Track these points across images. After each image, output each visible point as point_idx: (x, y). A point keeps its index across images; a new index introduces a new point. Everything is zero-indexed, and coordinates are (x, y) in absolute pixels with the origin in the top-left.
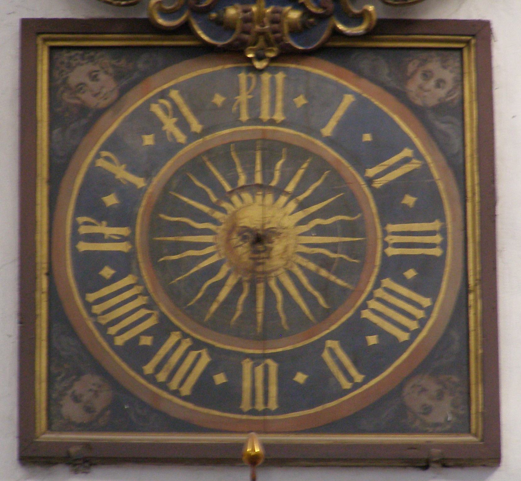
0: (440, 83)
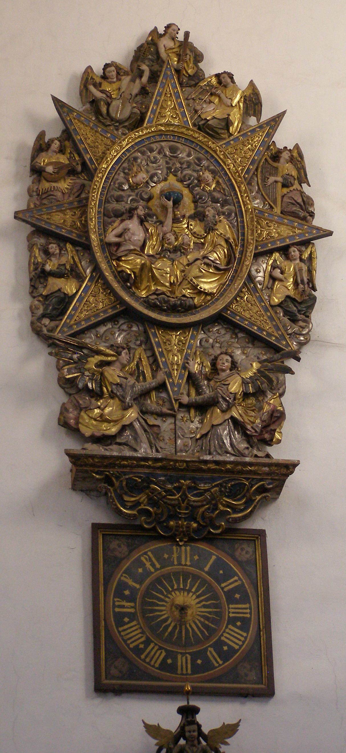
0: (247, 552)
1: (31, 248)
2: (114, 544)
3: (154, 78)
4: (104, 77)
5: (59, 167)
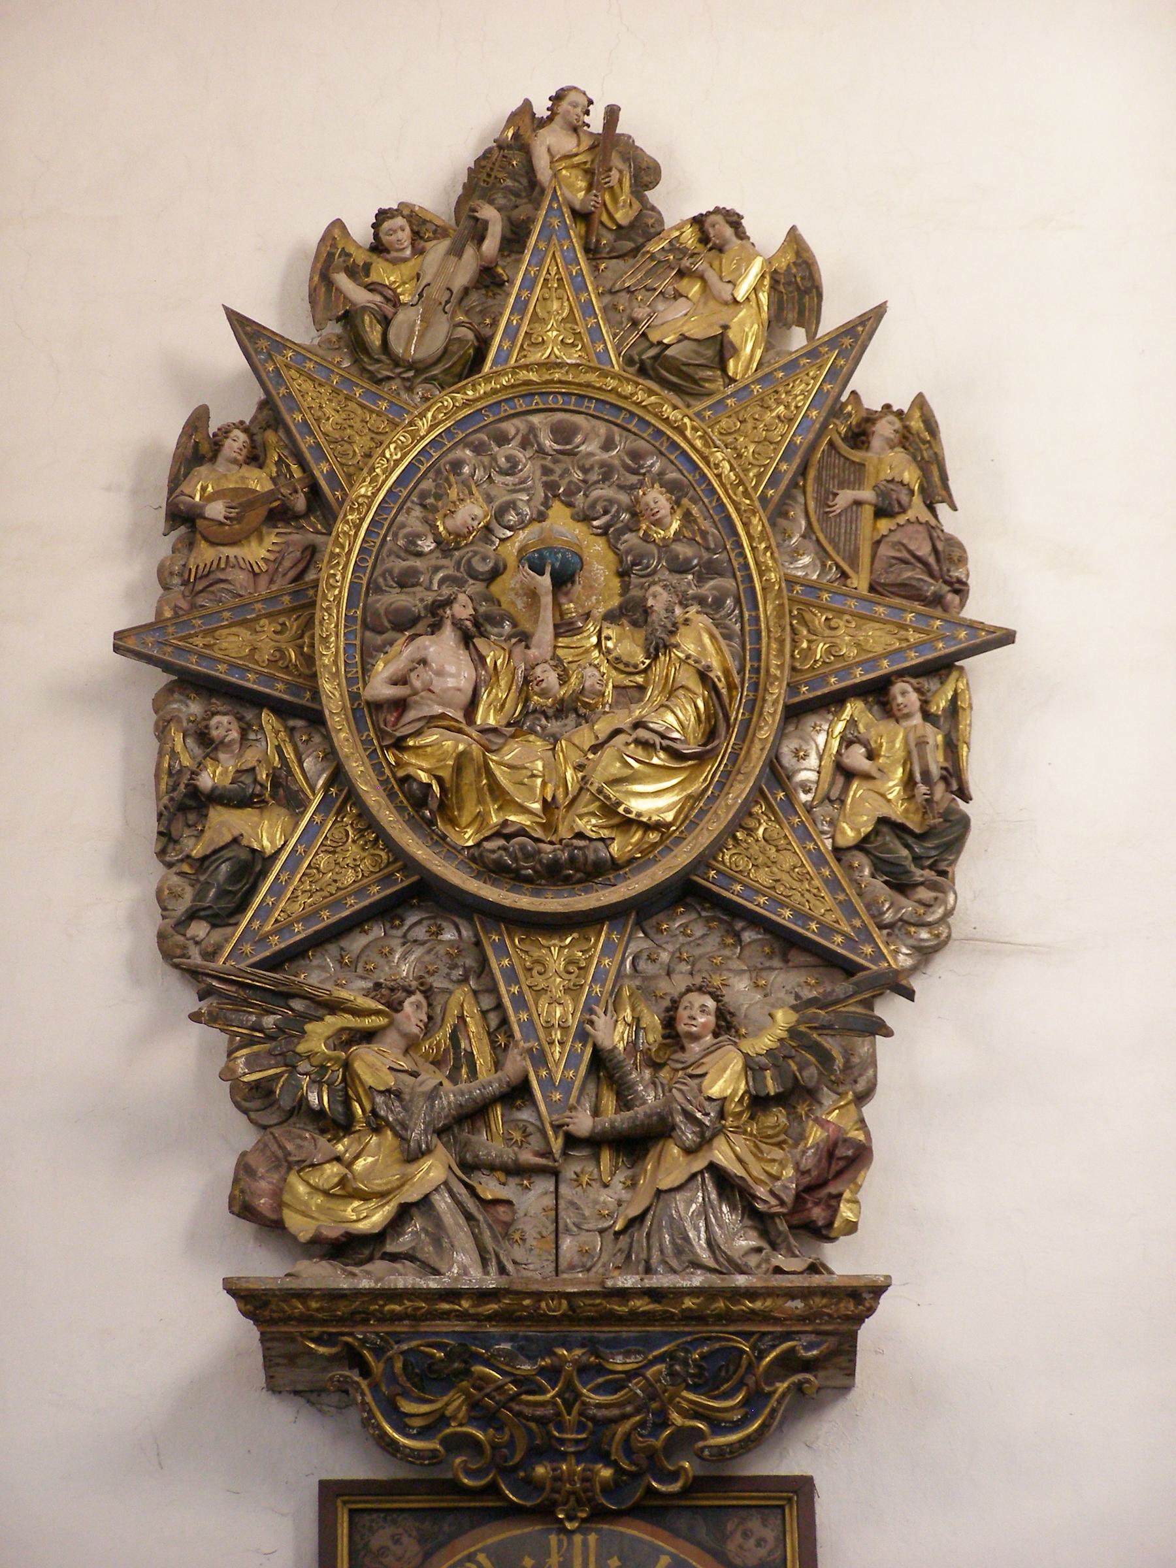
0: (760, 1542)
1: (161, 731)
2: (381, 1537)
3: (515, 240)
4: (378, 248)
5: (244, 502)
